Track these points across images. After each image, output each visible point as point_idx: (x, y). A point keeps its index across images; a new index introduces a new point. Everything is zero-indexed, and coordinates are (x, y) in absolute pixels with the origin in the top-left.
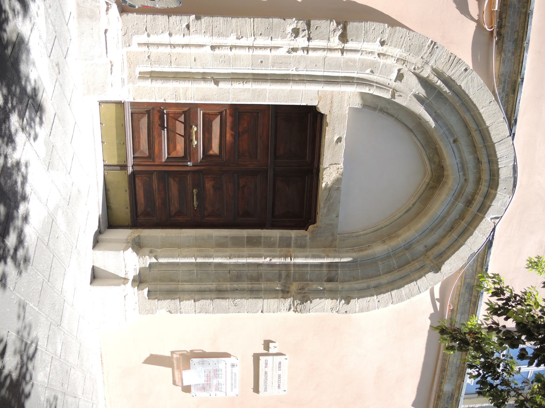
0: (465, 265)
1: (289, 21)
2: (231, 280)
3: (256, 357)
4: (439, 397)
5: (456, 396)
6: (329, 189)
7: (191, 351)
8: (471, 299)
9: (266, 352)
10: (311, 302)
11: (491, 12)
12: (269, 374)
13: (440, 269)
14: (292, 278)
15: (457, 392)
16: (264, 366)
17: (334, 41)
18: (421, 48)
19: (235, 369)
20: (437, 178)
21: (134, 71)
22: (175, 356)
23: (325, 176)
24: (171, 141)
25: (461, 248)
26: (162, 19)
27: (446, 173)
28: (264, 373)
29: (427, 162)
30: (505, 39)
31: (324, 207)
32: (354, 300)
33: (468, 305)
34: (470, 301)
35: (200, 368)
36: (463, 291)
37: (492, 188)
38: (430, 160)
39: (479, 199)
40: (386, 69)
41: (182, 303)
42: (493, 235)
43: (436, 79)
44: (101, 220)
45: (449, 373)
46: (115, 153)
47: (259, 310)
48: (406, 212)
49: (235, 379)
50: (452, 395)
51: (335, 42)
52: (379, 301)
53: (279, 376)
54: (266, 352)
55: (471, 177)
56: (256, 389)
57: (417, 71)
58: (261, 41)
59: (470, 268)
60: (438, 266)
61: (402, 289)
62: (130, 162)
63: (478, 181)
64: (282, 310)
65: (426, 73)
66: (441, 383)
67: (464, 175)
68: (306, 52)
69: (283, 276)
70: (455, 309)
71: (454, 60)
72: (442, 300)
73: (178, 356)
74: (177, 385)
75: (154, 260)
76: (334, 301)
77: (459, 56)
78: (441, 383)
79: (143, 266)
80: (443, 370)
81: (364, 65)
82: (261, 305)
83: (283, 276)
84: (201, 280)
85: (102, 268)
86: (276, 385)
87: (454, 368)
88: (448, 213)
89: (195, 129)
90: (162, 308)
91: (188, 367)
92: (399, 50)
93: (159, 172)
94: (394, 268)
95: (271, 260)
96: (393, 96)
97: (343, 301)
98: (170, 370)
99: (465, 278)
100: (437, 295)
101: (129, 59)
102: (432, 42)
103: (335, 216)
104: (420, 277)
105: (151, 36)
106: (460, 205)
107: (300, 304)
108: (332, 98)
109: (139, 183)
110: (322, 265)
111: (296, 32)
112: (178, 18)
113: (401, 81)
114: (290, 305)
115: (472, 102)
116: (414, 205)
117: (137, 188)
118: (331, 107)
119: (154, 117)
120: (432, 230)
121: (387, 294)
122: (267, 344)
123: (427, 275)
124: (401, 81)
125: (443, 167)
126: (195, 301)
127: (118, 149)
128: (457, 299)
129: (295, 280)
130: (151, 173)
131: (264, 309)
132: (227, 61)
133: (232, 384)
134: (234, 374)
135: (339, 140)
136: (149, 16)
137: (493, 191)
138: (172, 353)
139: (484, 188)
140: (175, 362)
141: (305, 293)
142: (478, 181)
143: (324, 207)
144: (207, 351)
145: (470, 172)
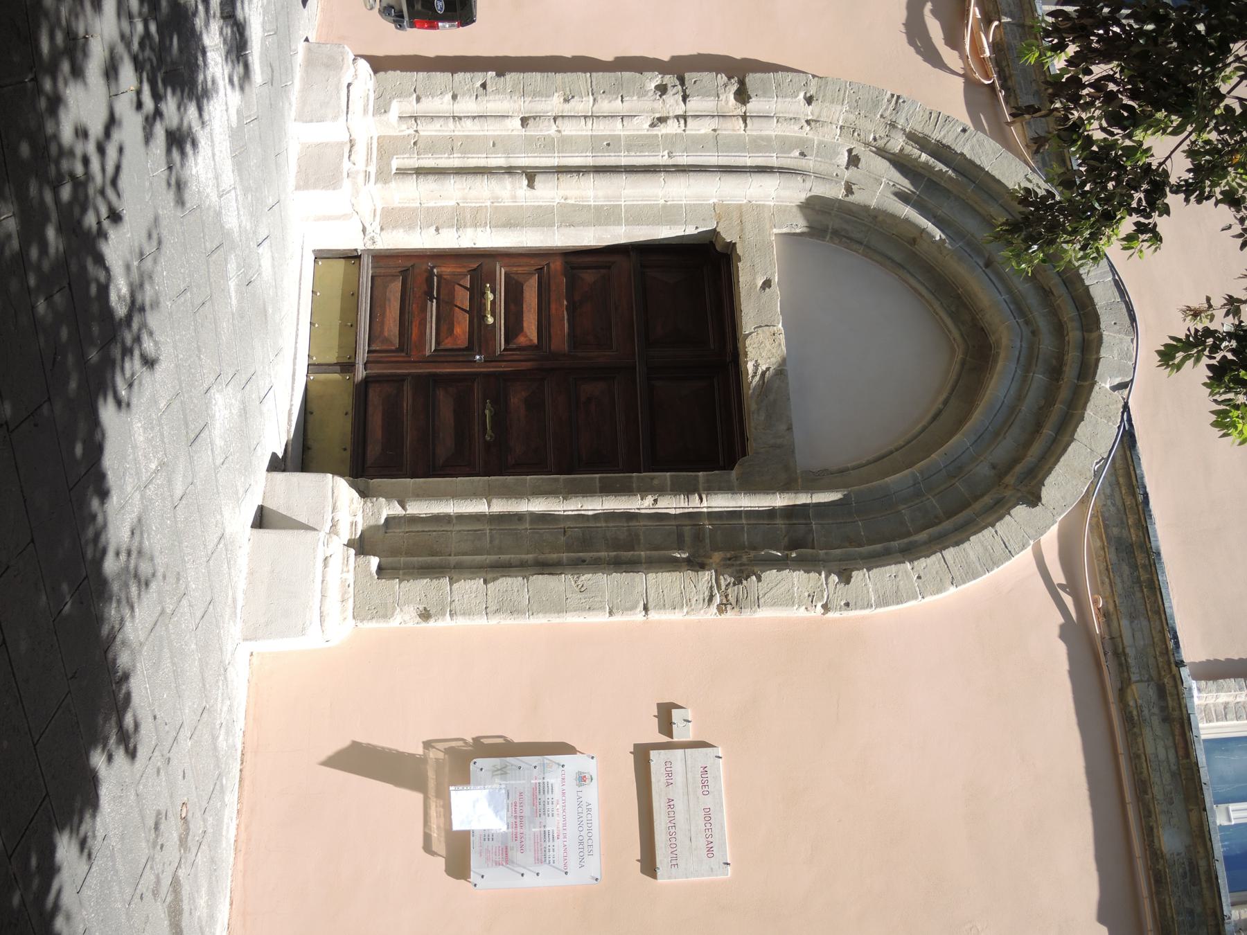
0: (1093, 484)
1: (648, 74)
2: (569, 548)
3: (642, 754)
4: (1158, 880)
5: (1202, 863)
6: (765, 385)
7: (477, 740)
8: (1139, 577)
9: (665, 739)
10: (759, 579)
11: (982, 62)
12: (679, 806)
13: (1039, 499)
14: (707, 541)
15: (1201, 850)
16: (663, 779)
17: (727, 102)
18: (876, 104)
19: (592, 793)
20: (977, 353)
21: (389, 164)
22: (432, 754)
23: (749, 349)
24: (445, 321)
25: (1070, 449)
26: (441, 78)
27: (992, 339)
28: (664, 804)
29: (948, 321)
30: (1018, 91)
31: (758, 410)
32: (861, 573)
33: (1139, 595)
34: (1138, 581)
35: (498, 784)
36: (1112, 556)
37: (1090, 331)
38: (954, 316)
39: (1072, 356)
40: (827, 150)
41: (456, 586)
42: (1130, 420)
43: (916, 152)
44: (290, 449)
45: (1157, 791)
46: (335, 342)
47: (637, 602)
48: (934, 418)
49: (589, 822)
50: (1193, 866)
51: (729, 98)
52: (919, 577)
53: (707, 811)
54: (665, 739)
55: (1042, 323)
56: (649, 866)
57: (881, 143)
58: (605, 106)
59: (1109, 502)
60: (1032, 494)
61: (966, 545)
62: (362, 357)
63: (1059, 330)
64: (693, 601)
65: (897, 143)
66: (1149, 833)
67: (1027, 323)
68: (682, 122)
69: (688, 539)
70: (1111, 608)
71: (936, 117)
72: (1073, 586)
73: (441, 755)
74: (433, 853)
75: (396, 510)
76: (814, 575)
77: (945, 113)
78: (1149, 833)
79: (372, 523)
80: (1142, 787)
81: (785, 144)
82: (640, 588)
83: (688, 539)
84: (500, 551)
85: (283, 511)
86: (702, 843)
87: (1167, 777)
88: (1020, 398)
89: (490, 296)
90: (407, 602)
91: (463, 778)
92: (839, 107)
93: (418, 377)
94: (936, 517)
95: (655, 501)
96: (849, 190)
97: (834, 578)
98: (418, 797)
99: (1106, 527)
100: (1058, 577)
101: (380, 147)
102: (893, 96)
103: (783, 427)
104: (1001, 518)
105: (423, 99)
106: (1039, 378)
107: (734, 584)
108: (741, 216)
109: (375, 397)
110: (771, 513)
111: (662, 89)
112: (468, 75)
113: (856, 166)
114: (711, 587)
115: (993, 178)
116: (945, 403)
117: (370, 409)
118: (742, 230)
119: (410, 281)
120: (996, 434)
121: (933, 558)
122: (665, 714)
123: (1013, 512)
124: (856, 166)
125: (982, 329)
126: (485, 582)
127: (340, 335)
128: (1107, 580)
129: (715, 548)
130: (399, 380)
131: (650, 600)
132: (548, 145)
133: (581, 843)
134: (585, 798)
135: (767, 284)
136: (421, 74)
137: (1094, 335)
138: (428, 745)
139: (1074, 335)
140: (431, 775)
141: (741, 565)
142: (1059, 330)
143: (758, 410)
144: (516, 741)
145: (1036, 313)
